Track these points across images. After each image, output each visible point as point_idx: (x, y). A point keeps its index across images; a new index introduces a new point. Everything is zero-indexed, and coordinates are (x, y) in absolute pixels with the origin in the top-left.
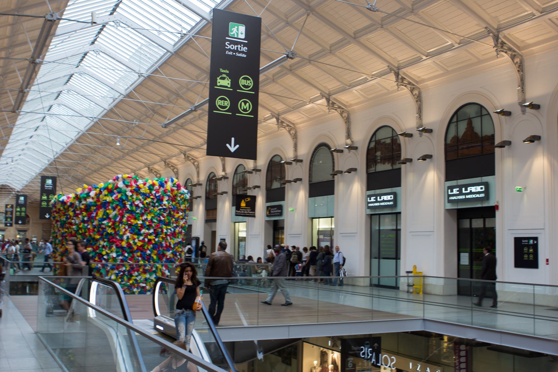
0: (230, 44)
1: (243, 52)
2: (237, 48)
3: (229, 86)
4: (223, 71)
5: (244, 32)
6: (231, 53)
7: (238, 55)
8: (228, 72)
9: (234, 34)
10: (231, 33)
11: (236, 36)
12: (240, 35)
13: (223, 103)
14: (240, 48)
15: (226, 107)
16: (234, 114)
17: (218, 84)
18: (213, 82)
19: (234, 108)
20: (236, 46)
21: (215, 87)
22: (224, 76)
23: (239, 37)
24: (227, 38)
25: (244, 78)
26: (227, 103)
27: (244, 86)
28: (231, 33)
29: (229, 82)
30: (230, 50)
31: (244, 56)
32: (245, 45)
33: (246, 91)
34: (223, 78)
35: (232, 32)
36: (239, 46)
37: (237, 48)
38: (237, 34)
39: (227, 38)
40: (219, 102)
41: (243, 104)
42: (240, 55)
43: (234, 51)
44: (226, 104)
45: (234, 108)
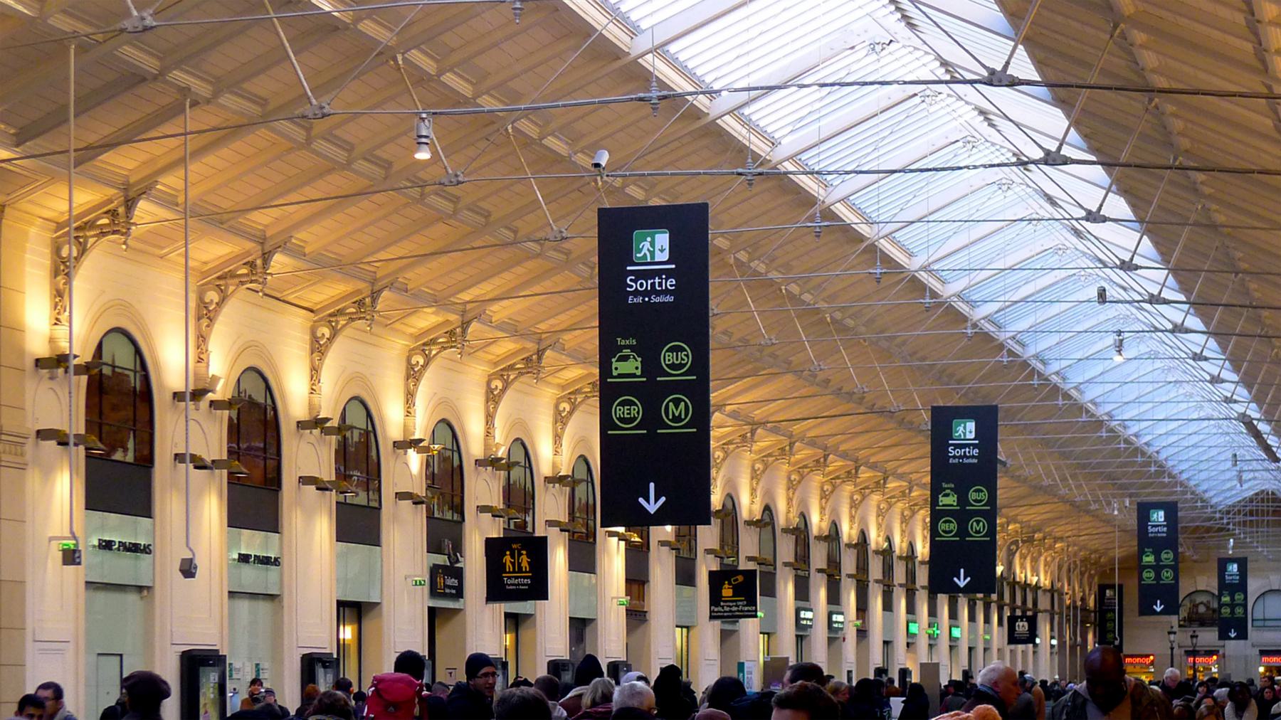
0: (954, 450)
1: (973, 457)
2: (965, 452)
3: (955, 504)
4: (946, 486)
5: (974, 430)
6: (956, 461)
7: (966, 461)
8: (953, 486)
9: (960, 435)
10: (957, 434)
11: (962, 437)
12: (968, 433)
13: (949, 527)
14: (969, 452)
15: (951, 531)
16: (962, 537)
17: (941, 504)
18: (934, 502)
19: (963, 531)
20: (963, 450)
21: (937, 508)
22: (948, 491)
23: (968, 437)
24: (950, 442)
25: (975, 491)
26: (953, 526)
27: (976, 501)
28: (957, 434)
29: (955, 498)
30: (954, 457)
31: (975, 461)
32: (975, 446)
33: (978, 506)
34: (947, 495)
35: (957, 432)
36: (967, 450)
37: (965, 452)
38: (965, 434)
39: (950, 442)
40: (942, 526)
41: (975, 523)
42: (970, 461)
43: (960, 457)
44: (952, 527)
45: (963, 531)
